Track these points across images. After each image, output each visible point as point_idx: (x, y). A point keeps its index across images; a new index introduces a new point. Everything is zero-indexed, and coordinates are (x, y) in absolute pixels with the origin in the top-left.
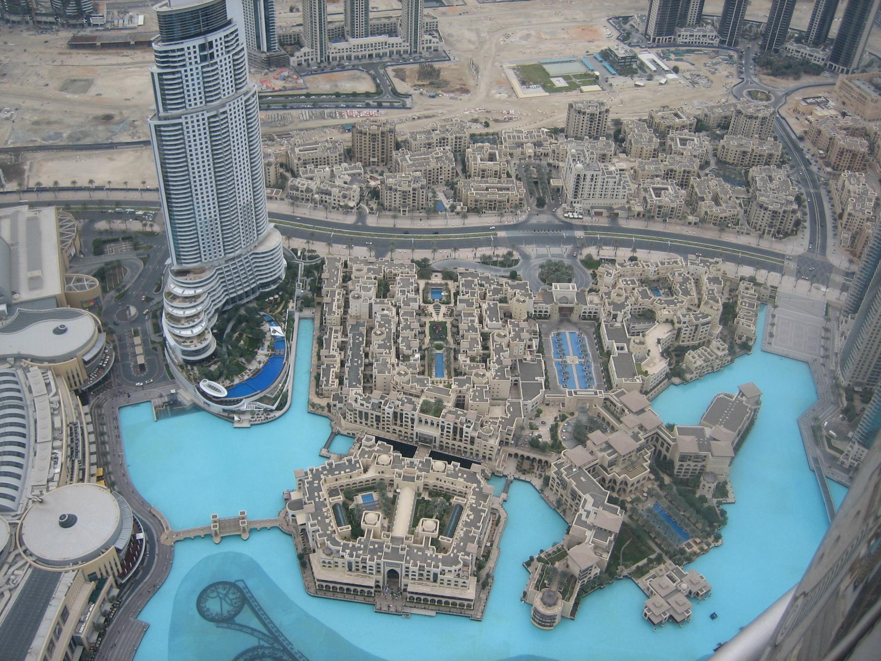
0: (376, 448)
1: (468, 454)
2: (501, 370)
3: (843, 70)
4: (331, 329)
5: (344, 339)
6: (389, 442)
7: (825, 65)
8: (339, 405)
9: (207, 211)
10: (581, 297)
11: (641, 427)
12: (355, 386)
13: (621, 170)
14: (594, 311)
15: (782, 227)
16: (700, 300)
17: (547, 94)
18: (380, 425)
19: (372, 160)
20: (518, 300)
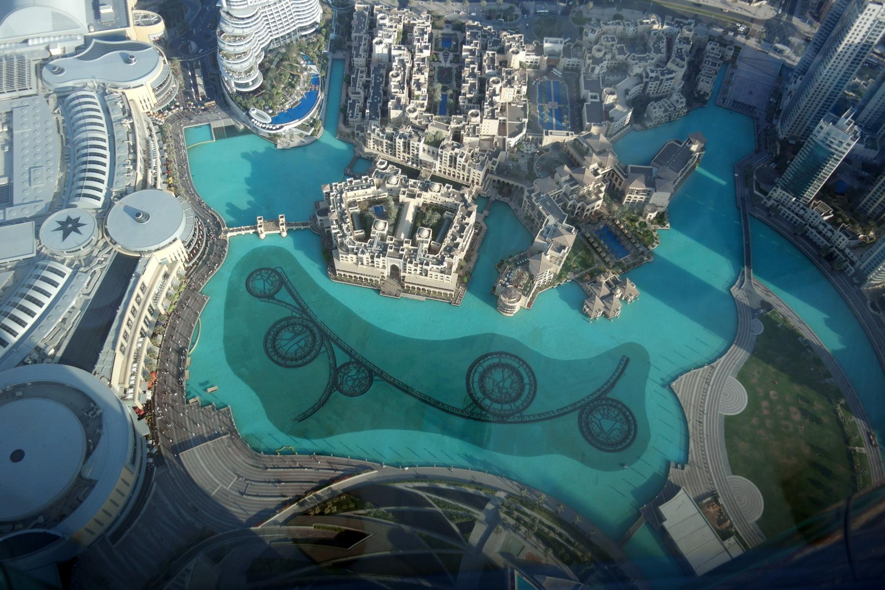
1: (461, 178)
2: (493, 111)
4: (358, 70)
5: (368, 79)
6: (398, 165)
8: (361, 134)
10: (567, 52)
12: (374, 119)
14: (576, 64)
16: (669, 58)
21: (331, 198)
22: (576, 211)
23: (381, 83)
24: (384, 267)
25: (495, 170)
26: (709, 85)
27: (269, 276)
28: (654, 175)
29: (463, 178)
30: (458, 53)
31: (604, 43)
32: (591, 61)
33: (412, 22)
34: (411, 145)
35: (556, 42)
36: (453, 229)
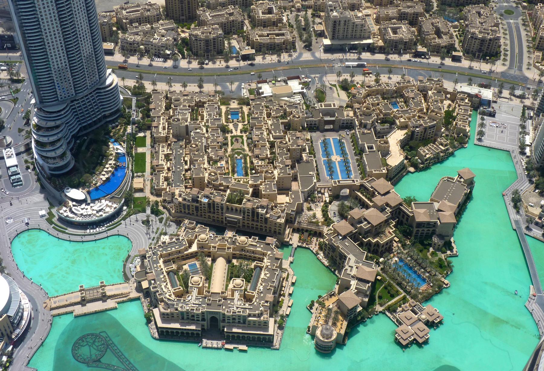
0: (197, 230)
1: (264, 230)
5: (169, 152)
9: (59, 63)
11: (387, 205)
12: (179, 186)
13: (366, 15)
15: (488, 51)
18: (199, 214)
19: (181, 18)
24: (203, 320)
27: (94, 341)
29: (266, 230)
34: (216, 205)
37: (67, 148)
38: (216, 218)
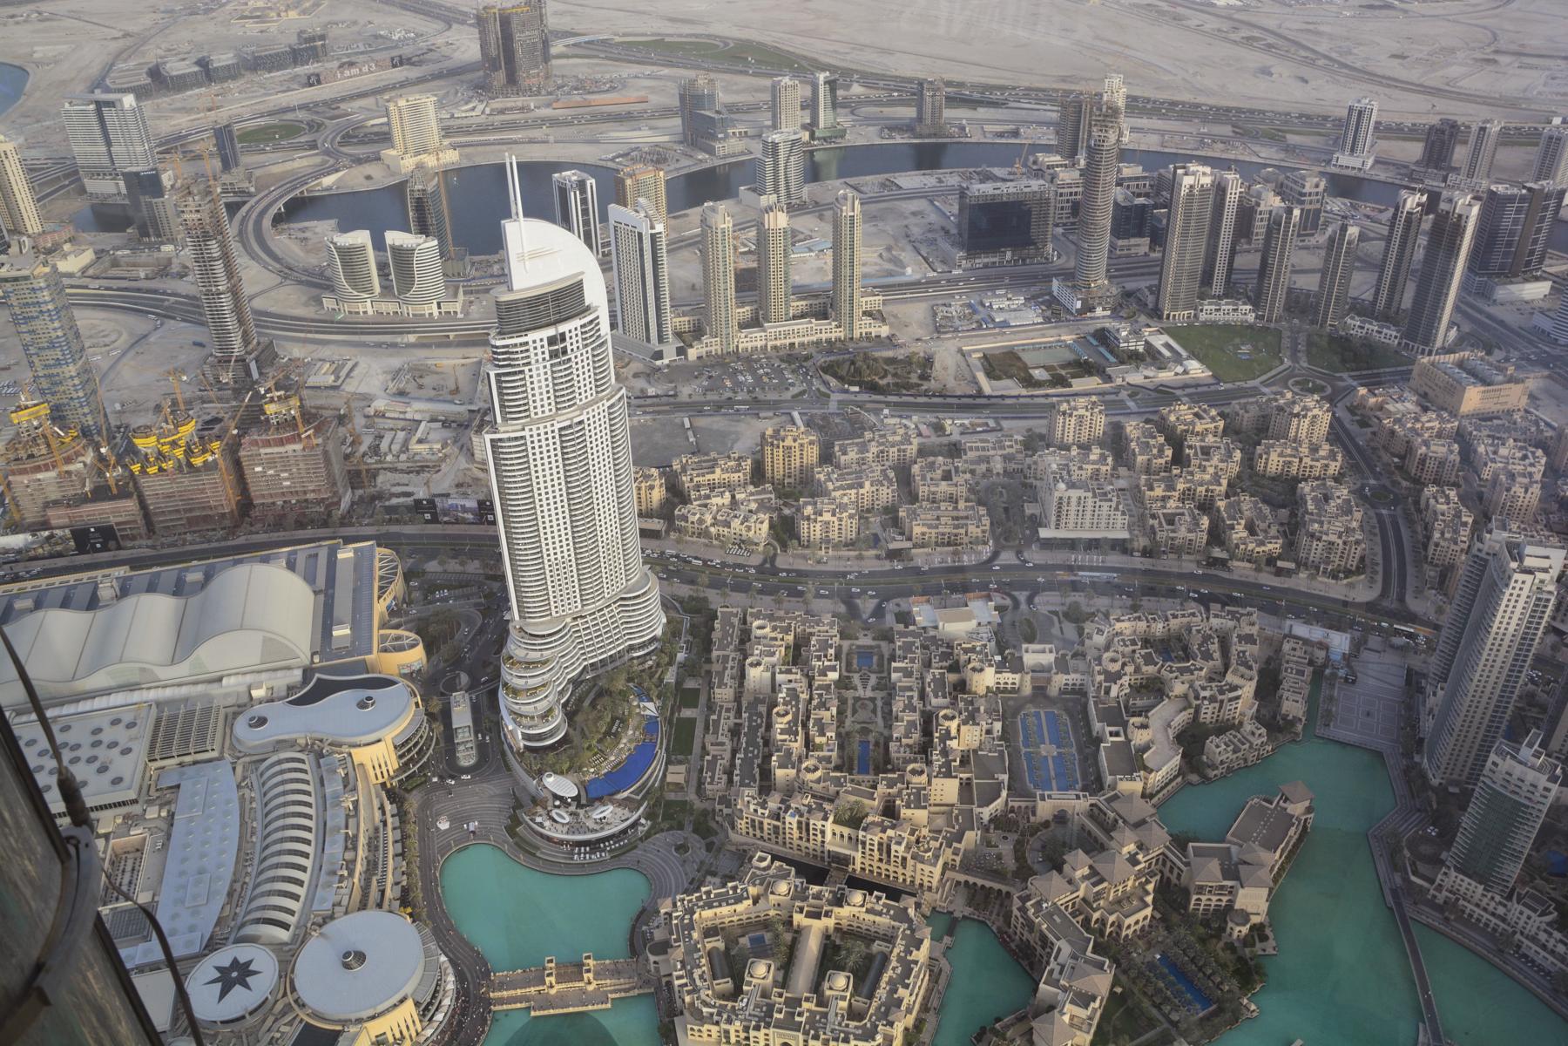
1: (901, 880)
2: (947, 764)
3: (1423, 350)
4: (721, 707)
5: (738, 721)
7: (1399, 344)
8: (726, 811)
10: (1062, 665)
12: (748, 786)
14: (1078, 682)
16: (1226, 667)
17: (1024, 392)
20: (974, 669)
21: (675, 922)
22: (1108, 930)
23: (760, 726)
25: (958, 863)
26: (1298, 705)
28: (1235, 859)
29: (904, 880)
30: (885, 675)
31: (1120, 649)
32: (1102, 677)
33: (808, 630)
35: (1043, 651)
36: (890, 972)
37: (558, 701)
38: (811, 851)
